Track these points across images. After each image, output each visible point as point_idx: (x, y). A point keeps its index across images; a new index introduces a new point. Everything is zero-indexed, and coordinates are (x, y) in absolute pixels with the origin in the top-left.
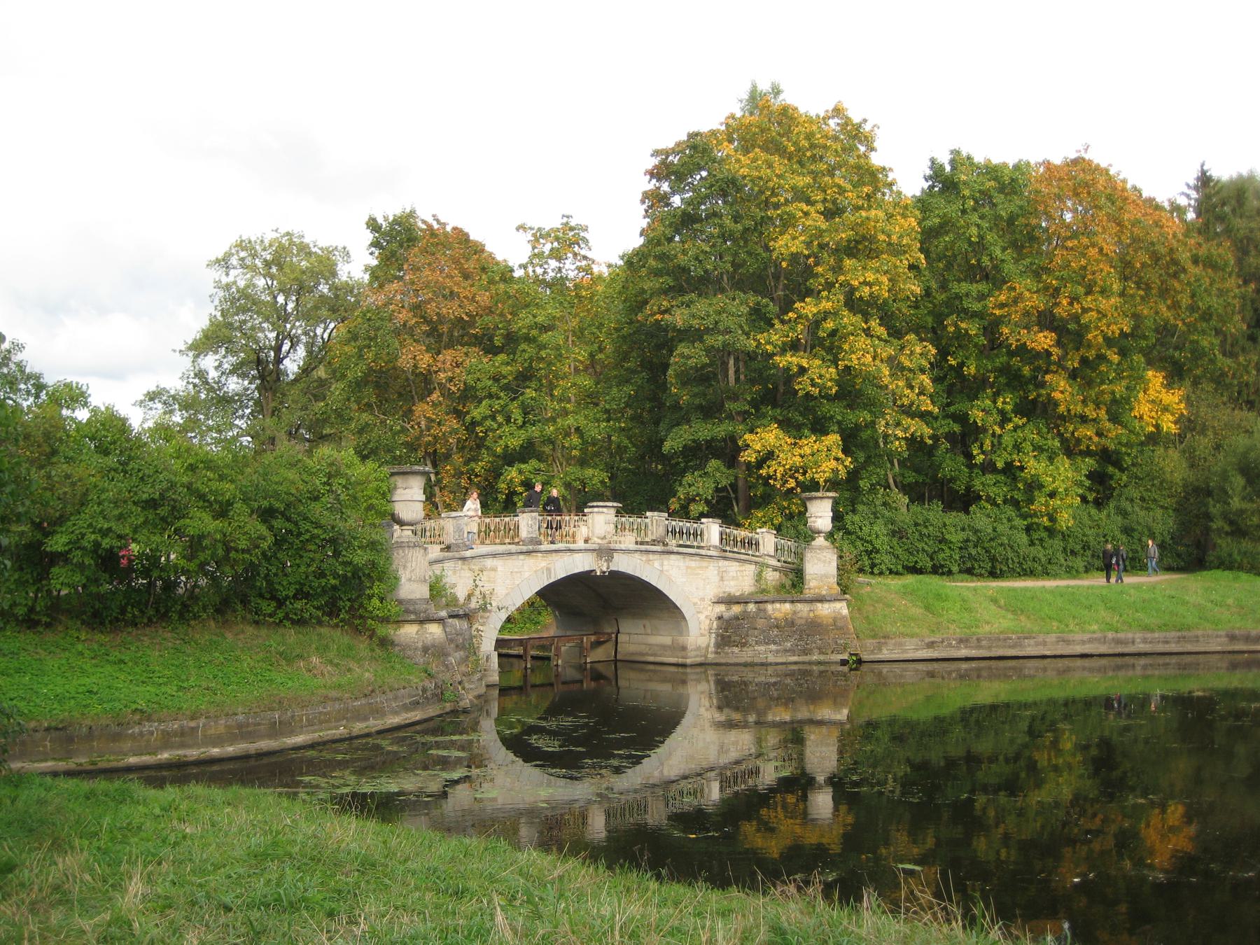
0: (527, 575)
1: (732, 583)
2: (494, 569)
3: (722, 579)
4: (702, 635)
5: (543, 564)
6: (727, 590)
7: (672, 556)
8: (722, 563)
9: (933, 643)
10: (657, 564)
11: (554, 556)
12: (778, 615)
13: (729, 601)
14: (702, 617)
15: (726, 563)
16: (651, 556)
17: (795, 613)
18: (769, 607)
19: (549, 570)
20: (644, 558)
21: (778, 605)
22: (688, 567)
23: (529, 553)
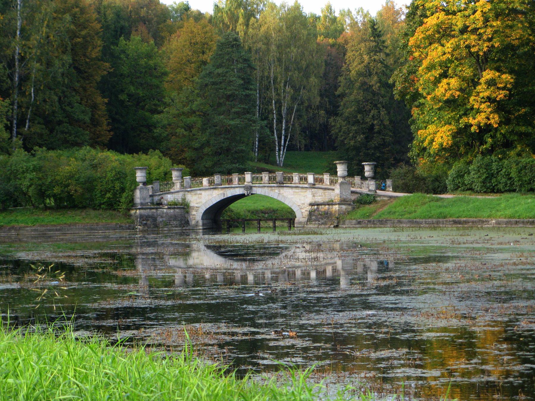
0: (214, 196)
1: (319, 198)
2: (201, 194)
3: (314, 196)
4: (303, 217)
5: (220, 192)
6: (317, 200)
7: (285, 188)
8: (313, 190)
9: (360, 221)
10: (277, 191)
11: (226, 190)
12: (323, 210)
13: (311, 205)
14: (303, 211)
15: (316, 190)
16: (273, 188)
17: (329, 209)
18: (320, 207)
19: (224, 194)
20: (270, 189)
21: (323, 206)
22: (294, 192)
23: (215, 188)
